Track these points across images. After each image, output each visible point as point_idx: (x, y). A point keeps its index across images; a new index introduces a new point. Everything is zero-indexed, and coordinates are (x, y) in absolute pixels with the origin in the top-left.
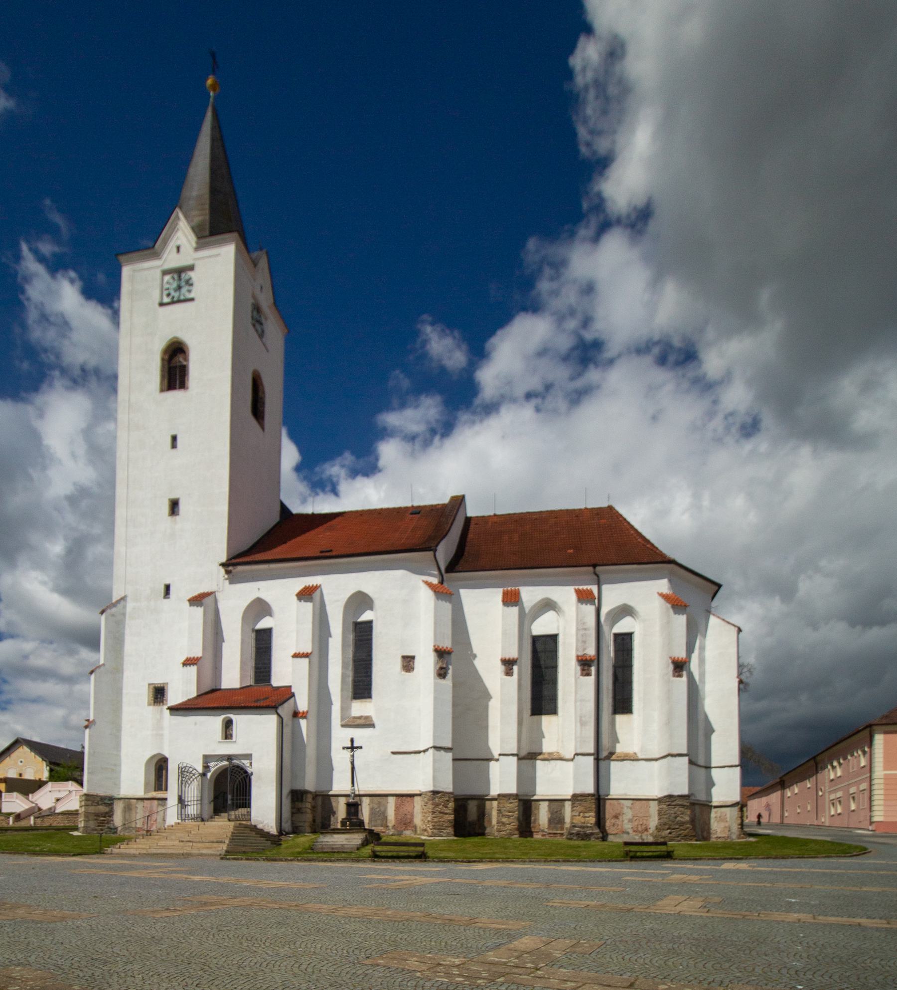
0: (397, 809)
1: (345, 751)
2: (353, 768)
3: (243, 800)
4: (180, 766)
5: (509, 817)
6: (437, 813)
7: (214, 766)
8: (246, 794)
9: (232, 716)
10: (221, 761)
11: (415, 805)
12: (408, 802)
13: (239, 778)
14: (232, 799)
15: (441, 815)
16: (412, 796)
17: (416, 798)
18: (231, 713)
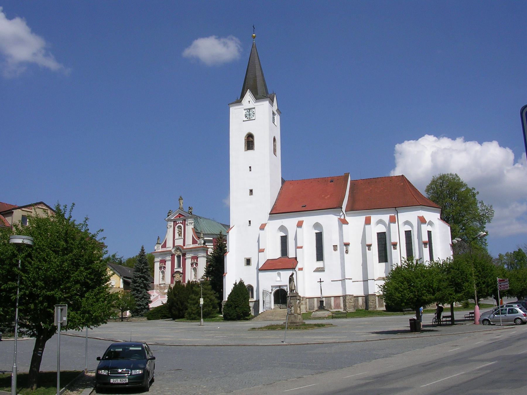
15: (350, 303)
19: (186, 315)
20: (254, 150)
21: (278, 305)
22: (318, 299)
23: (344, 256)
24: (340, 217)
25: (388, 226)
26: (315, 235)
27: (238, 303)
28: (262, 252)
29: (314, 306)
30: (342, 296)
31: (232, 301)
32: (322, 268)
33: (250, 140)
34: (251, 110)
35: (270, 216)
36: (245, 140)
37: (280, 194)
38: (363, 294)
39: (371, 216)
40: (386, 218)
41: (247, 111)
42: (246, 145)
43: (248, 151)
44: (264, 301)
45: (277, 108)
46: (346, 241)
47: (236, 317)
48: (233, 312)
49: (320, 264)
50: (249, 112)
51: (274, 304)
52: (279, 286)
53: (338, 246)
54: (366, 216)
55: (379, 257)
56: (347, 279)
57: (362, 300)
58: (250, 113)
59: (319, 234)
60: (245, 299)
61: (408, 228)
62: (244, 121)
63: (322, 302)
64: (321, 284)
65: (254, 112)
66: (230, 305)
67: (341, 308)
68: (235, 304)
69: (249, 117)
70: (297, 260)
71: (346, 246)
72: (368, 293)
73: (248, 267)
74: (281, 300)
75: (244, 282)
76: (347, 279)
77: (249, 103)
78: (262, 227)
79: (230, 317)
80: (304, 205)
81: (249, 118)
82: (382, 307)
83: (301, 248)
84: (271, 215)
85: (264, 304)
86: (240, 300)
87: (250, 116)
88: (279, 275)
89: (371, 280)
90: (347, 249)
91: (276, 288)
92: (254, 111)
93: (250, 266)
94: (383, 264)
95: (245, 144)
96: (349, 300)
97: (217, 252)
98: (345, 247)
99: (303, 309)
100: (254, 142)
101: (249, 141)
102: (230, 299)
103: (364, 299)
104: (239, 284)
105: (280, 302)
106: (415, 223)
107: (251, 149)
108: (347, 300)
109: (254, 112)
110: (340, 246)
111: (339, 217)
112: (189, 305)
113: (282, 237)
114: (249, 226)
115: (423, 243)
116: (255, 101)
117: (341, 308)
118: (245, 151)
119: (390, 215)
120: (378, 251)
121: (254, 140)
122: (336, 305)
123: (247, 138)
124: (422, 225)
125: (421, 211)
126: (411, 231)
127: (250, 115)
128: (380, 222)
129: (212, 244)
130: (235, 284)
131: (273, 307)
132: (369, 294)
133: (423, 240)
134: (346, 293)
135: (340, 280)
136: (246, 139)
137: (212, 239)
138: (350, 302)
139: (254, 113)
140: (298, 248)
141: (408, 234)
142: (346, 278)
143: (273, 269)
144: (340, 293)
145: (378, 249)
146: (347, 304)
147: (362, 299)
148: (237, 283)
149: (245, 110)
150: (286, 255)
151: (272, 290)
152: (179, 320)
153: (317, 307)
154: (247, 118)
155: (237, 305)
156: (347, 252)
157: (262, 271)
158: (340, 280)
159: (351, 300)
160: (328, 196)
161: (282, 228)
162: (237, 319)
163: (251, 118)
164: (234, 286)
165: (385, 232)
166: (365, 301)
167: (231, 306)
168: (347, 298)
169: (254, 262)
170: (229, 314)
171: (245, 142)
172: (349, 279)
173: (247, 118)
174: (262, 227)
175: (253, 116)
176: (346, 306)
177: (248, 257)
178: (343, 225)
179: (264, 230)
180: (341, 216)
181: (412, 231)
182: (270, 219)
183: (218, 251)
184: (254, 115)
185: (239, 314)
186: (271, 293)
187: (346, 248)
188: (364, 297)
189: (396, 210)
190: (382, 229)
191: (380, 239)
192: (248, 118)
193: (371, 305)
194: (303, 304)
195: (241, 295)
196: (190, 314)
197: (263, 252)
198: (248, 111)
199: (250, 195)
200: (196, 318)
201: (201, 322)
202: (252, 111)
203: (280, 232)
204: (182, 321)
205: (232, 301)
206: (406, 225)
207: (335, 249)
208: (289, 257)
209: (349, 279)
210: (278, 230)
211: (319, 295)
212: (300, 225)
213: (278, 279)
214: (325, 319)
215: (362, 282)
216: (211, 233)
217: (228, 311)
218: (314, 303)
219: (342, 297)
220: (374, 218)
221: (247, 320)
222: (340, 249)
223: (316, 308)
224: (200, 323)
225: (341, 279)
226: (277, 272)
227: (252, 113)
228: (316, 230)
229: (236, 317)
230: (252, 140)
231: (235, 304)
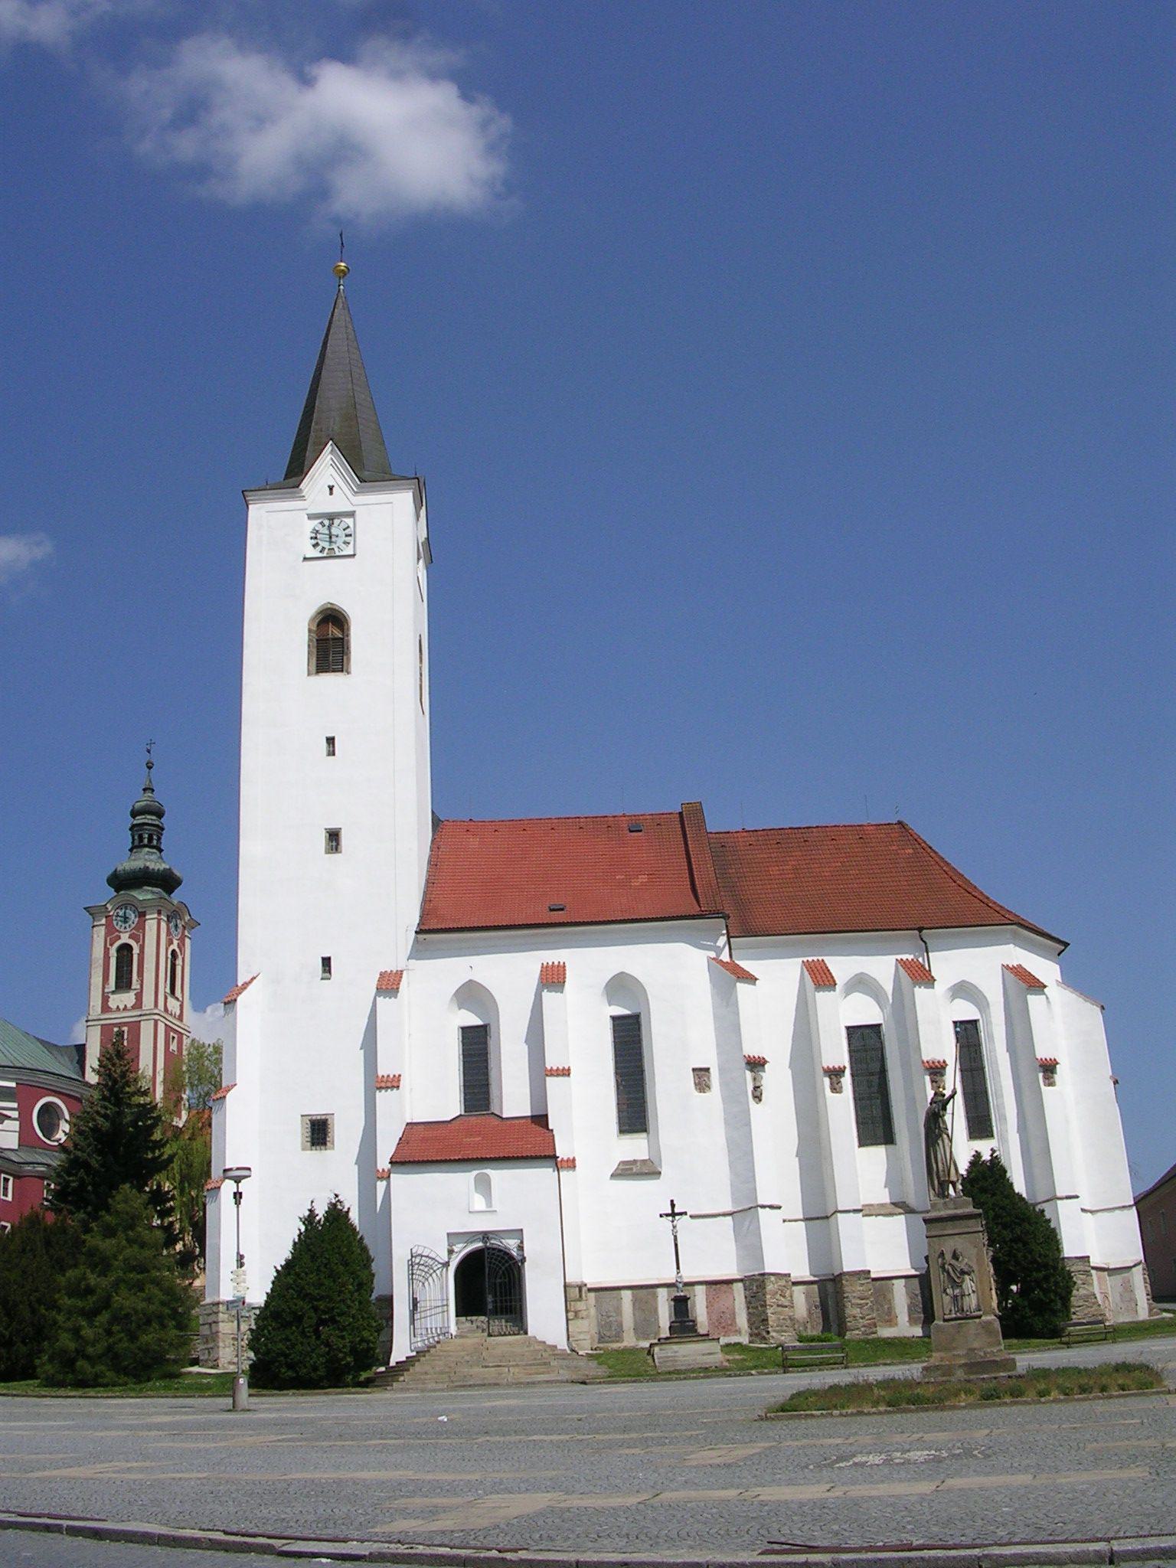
0: (709, 1305)
1: (664, 1218)
2: (676, 1245)
3: (506, 1302)
4: (414, 1251)
5: (861, 1306)
6: (775, 1306)
7: (462, 1250)
8: (501, 1288)
9: (488, 1171)
10: (471, 1242)
11: (736, 1295)
12: (725, 1292)
13: (503, 1268)
14: (495, 1302)
15: (780, 1309)
16: (729, 1282)
17: (735, 1284)
18: (486, 1168)
19: (45, 1365)
20: (348, 673)
21: (472, 1322)
22: (635, 1292)
23: (748, 1111)
24: (718, 955)
25: (891, 1001)
26: (608, 1025)
27: (331, 1305)
28: (393, 1087)
29: (620, 1325)
30: (741, 1280)
31: (304, 1295)
32: (644, 1161)
33: (330, 636)
34: (336, 522)
35: (416, 940)
36: (310, 631)
37: (434, 864)
38: (808, 1273)
39: (825, 958)
40: (882, 967)
41: (321, 523)
42: (315, 650)
43: (321, 674)
44: (415, 1303)
45: (426, 536)
46: (751, 1050)
47: (322, 1372)
48: (309, 1349)
49: (635, 1147)
50: (329, 527)
51: (457, 1316)
52: (481, 1236)
53: (711, 1070)
54: (805, 959)
55: (860, 1123)
56: (763, 1207)
57: (806, 1297)
58: (334, 531)
59: (631, 1021)
60: (360, 1286)
61: (967, 1011)
62: (305, 559)
63: (681, 1305)
64: (674, 1227)
65: (348, 527)
66: (294, 1313)
67: (739, 1332)
68: (316, 1309)
69: (326, 545)
70: (550, 1128)
71: (752, 1071)
72: (842, 1270)
73: (317, 1154)
74: (495, 1296)
75: (348, 1212)
76: (763, 1207)
77: (331, 494)
78: (389, 985)
79: (290, 1373)
80: (557, 902)
81: (326, 551)
82: (891, 1326)
83: (564, 1075)
84: (421, 937)
85: (417, 1316)
86: (340, 1292)
87: (331, 542)
88: (484, 1186)
89: (851, 1214)
90: (758, 1084)
91: (468, 1242)
92: (351, 526)
93: (328, 1152)
94: (879, 1152)
95: (309, 646)
96: (778, 1296)
97: (103, 1111)
98: (749, 1074)
99: (582, 1337)
100: (348, 642)
101: (328, 639)
102: (289, 1287)
103: (817, 1295)
104: (326, 1219)
105: (490, 1306)
106: (993, 990)
107: (334, 671)
108: (768, 1297)
109: (348, 527)
110: (721, 1070)
111: (713, 954)
112: (60, 1318)
113: (465, 1030)
114: (322, 979)
115: (1040, 1066)
116: (358, 486)
117: (739, 1332)
118: (309, 675)
119: (899, 957)
120: (855, 1099)
121: (347, 636)
122: (714, 1317)
123: (318, 625)
124: (1029, 997)
125: (1012, 946)
126: (975, 1022)
127: (334, 539)
128: (862, 983)
129: (15, 1105)
130: (310, 1220)
131: (453, 1330)
132: (845, 1270)
133: (1039, 1057)
134: (764, 1269)
135: (724, 1215)
136: (314, 628)
137: (13, 1085)
138: (778, 1306)
139: (348, 532)
140: (552, 1075)
141: (968, 1034)
142: (760, 1202)
143: (459, 1161)
144: (728, 1267)
145: (854, 1092)
146: (769, 1311)
147: (808, 1295)
148: (316, 1212)
149: (311, 517)
150: (487, 1106)
151: (451, 1252)
152: (8, 1388)
153: (632, 1326)
154: (319, 548)
155: (325, 1312)
156: (758, 1094)
157: (402, 1168)
158: (724, 1215)
159: (784, 1297)
160: (643, 878)
161: (471, 994)
162: (325, 1383)
163: (336, 549)
164: (303, 1228)
165: (879, 1025)
166: (818, 1304)
167: (299, 1319)
168: (770, 1287)
169: (346, 1134)
170: (286, 1356)
171: (310, 640)
172: (771, 1207)
173: (319, 548)
174: (389, 985)
175: (347, 543)
176: (765, 1320)
177: (318, 1110)
178: (738, 984)
179: (399, 994)
180: (719, 951)
181: (981, 1024)
182: (418, 952)
183: (106, 1108)
184: (348, 539)
185: (341, 1355)
186: (446, 1265)
187: (755, 1079)
188: (815, 1287)
189: (922, 939)
190: (865, 1011)
191: (858, 1051)
192: (324, 548)
193: (854, 1317)
194: (580, 1314)
195: (342, 1268)
196: (67, 1362)
197: (398, 1087)
198: (327, 522)
199: (327, 852)
200: (100, 1380)
201: (233, 1396)
202: (343, 526)
203: (460, 1009)
204: (30, 1393)
205: (304, 1295)
206: (958, 1001)
207: (699, 1084)
208: (504, 1116)
209: (771, 1207)
210: (452, 999)
211: (670, 1276)
212: (553, 978)
213: (479, 1203)
214: (753, 1372)
215: (803, 1224)
216: (11, 1065)
217: (280, 1345)
218: (618, 1310)
219: (740, 1285)
220: (842, 966)
221: (367, 1383)
222: (724, 1084)
223: (665, 1333)
224: (231, 1400)
225: (729, 1208)
226: (475, 1173)
227: (342, 533)
228: (613, 1007)
229: (322, 1372)
230: (341, 636)
231: (316, 1309)
